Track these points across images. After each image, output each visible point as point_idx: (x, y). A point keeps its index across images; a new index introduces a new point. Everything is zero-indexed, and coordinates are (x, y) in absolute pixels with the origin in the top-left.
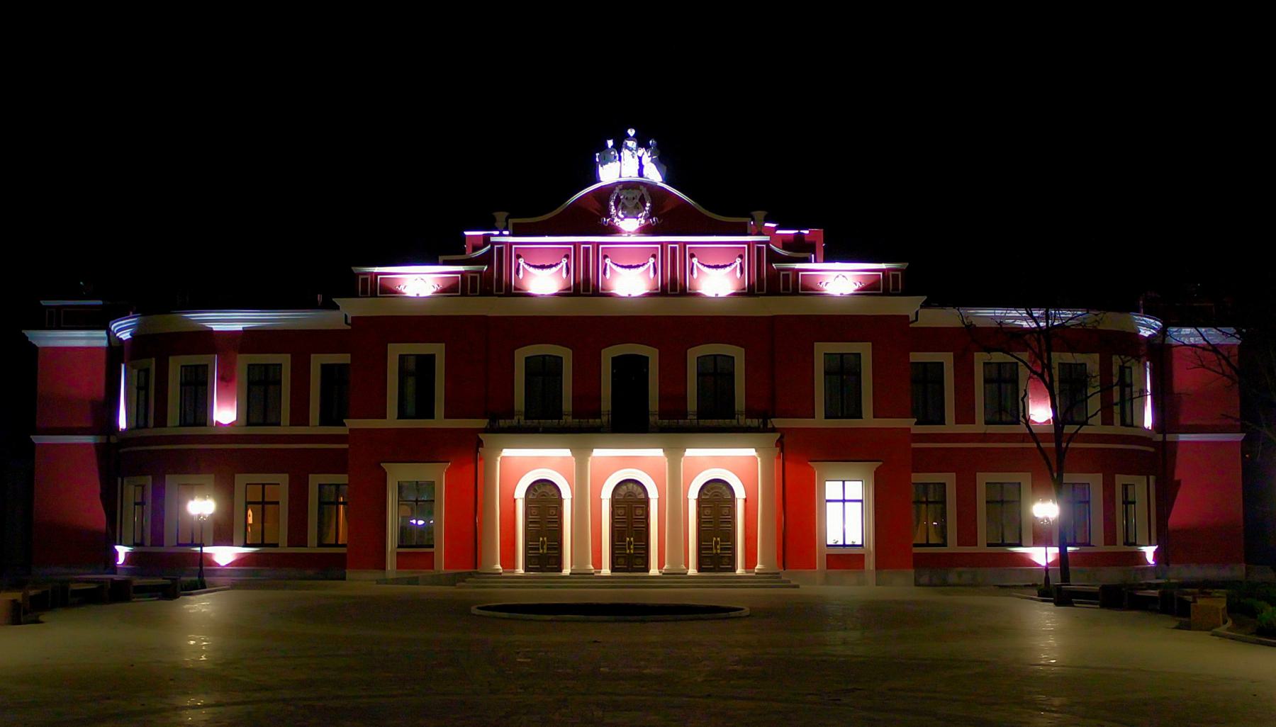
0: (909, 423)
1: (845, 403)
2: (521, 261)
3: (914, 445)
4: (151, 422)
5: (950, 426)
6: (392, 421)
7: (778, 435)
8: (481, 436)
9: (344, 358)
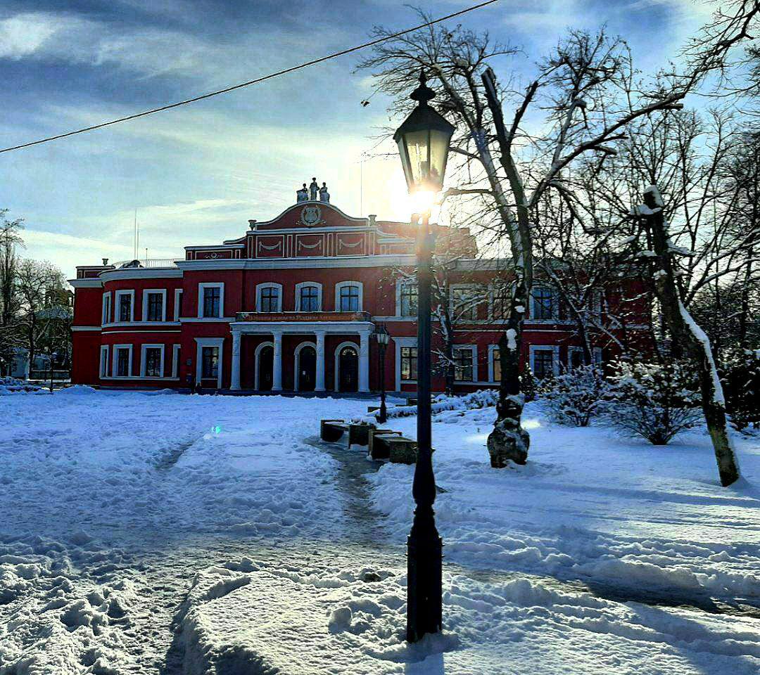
6: (200, 319)
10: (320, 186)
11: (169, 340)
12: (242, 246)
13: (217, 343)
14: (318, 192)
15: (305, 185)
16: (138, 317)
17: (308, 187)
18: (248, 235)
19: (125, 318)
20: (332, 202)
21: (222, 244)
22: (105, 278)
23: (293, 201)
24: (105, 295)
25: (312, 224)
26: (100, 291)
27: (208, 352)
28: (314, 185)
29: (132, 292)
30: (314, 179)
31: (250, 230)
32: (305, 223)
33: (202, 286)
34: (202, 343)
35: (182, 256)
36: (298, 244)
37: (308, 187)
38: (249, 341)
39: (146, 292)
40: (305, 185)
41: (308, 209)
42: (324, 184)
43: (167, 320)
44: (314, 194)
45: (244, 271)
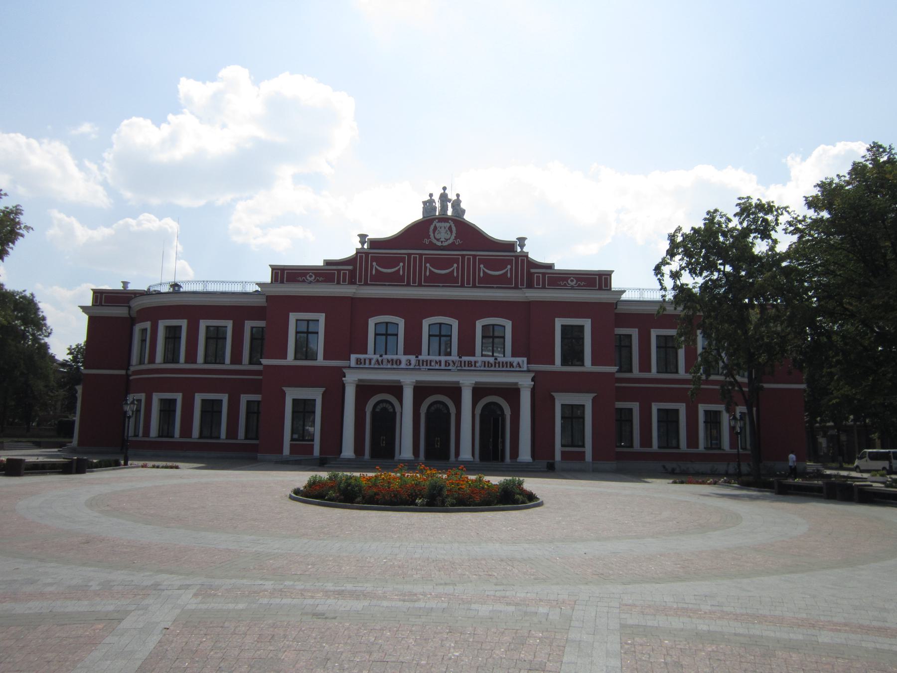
0: (613, 369)
1: (573, 354)
2: (374, 264)
3: (617, 385)
4: (146, 361)
5: (636, 373)
6: (291, 359)
7: (533, 375)
8: (344, 370)
9: (261, 324)
10: (452, 196)
11: (235, 388)
12: (350, 267)
13: (315, 394)
14: (449, 205)
15: (431, 195)
16: (191, 357)
17: (436, 198)
18: (357, 253)
19: (172, 355)
20: (468, 217)
21: (321, 264)
22: (136, 304)
23: (417, 215)
24: (138, 328)
25: (445, 244)
26: (131, 321)
27: (303, 409)
28: (444, 198)
29: (184, 323)
30: (445, 189)
31: (360, 246)
32: (435, 241)
33: (293, 317)
34: (292, 394)
35: (267, 278)
36: (426, 268)
37: (436, 198)
38: (365, 390)
39: (203, 324)
40: (431, 195)
41: (438, 225)
42: (458, 195)
43: (232, 363)
44: (444, 208)
45: (353, 301)
